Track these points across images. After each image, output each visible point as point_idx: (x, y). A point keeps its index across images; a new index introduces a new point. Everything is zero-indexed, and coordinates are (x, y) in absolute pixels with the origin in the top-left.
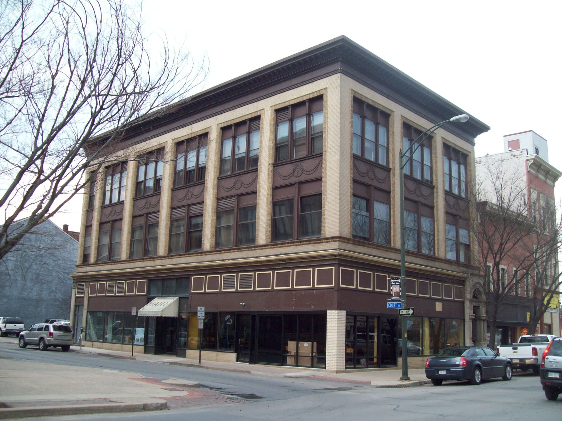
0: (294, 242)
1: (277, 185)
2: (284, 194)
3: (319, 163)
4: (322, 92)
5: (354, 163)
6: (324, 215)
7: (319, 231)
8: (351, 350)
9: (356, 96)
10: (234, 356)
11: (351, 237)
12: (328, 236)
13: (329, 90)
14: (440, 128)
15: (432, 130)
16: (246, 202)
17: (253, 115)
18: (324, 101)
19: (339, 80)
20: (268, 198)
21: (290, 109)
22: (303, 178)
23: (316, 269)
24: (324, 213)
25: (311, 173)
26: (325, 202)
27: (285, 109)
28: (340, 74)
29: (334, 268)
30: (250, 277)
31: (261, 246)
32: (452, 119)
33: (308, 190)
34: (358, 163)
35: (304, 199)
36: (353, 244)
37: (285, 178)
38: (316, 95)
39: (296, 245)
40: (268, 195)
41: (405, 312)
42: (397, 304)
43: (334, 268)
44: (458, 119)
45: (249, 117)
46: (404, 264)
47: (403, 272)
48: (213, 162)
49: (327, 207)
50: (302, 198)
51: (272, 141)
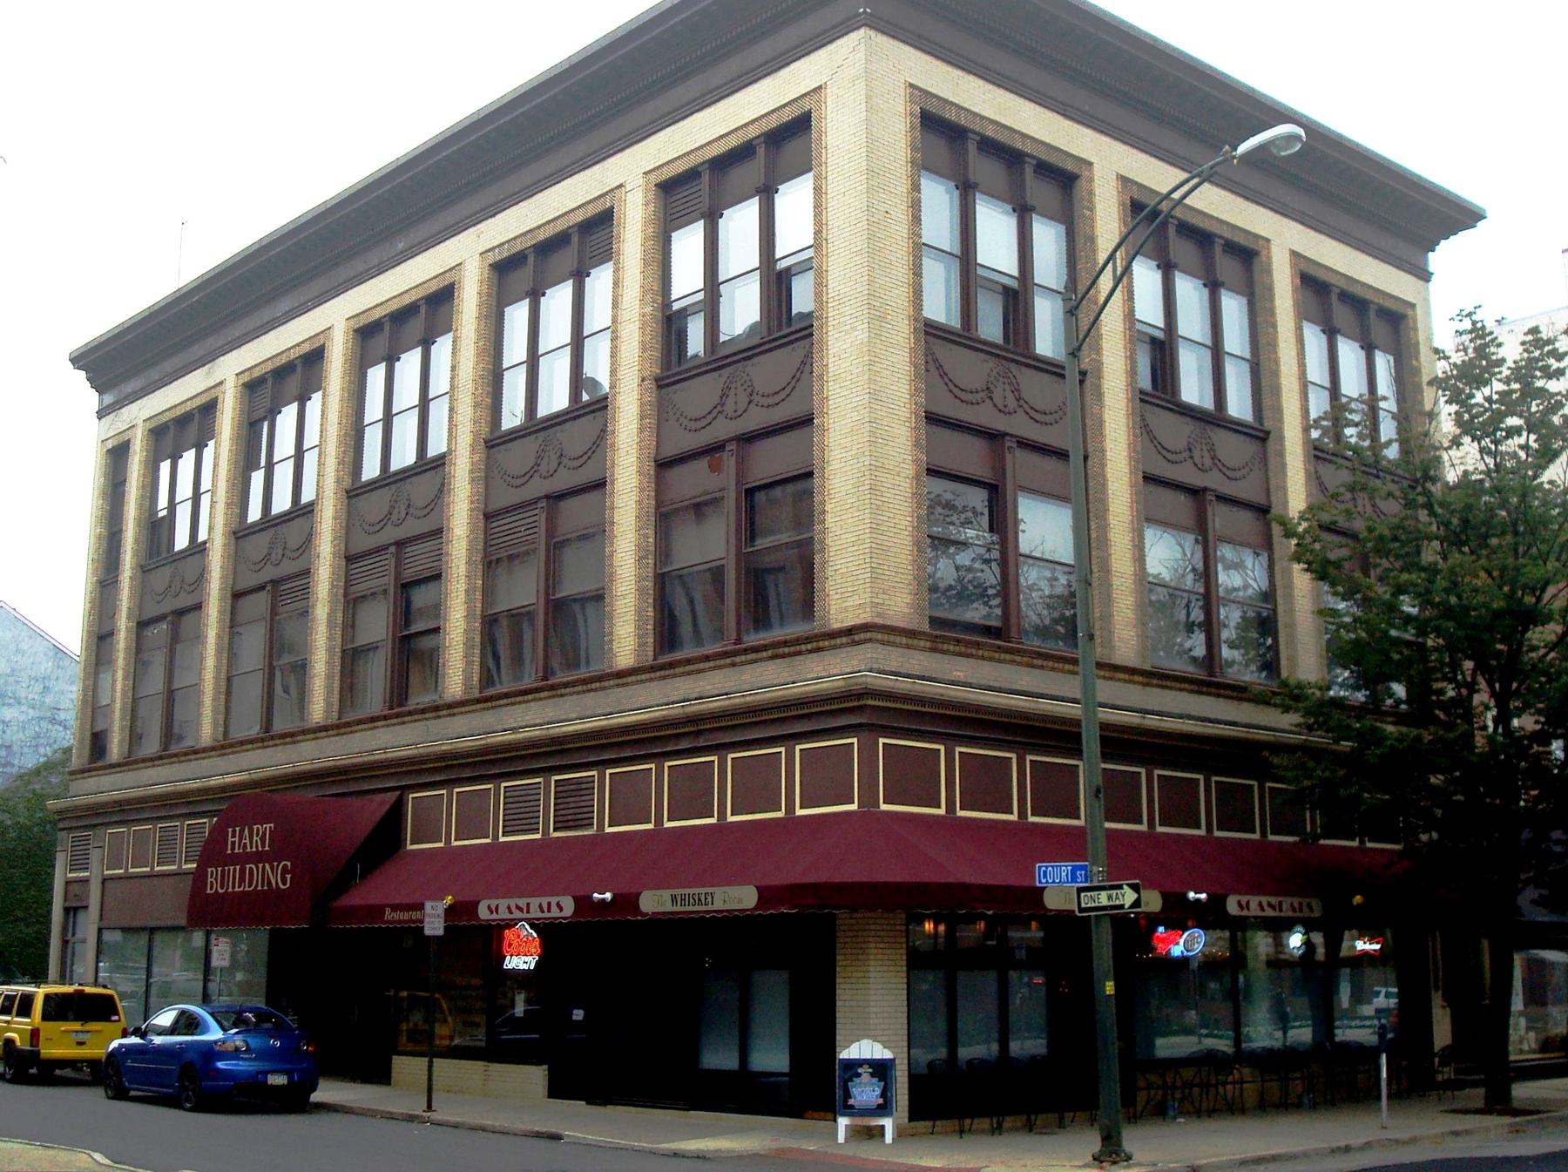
0: (726, 655)
1: (670, 451)
2: (693, 480)
3: (803, 363)
4: (807, 105)
5: (929, 354)
6: (823, 550)
7: (807, 605)
8: (71, 1015)
9: (933, 108)
10: (536, 1076)
11: (926, 627)
12: (836, 625)
13: (830, 95)
14: (1206, 185)
15: (1176, 195)
16: (574, 513)
17: (591, 211)
18: (814, 135)
19: (861, 55)
20: (640, 502)
21: (706, 177)
22: (756, 419)
23: (798, 748)
24: (822, 542)
25: (777, 399)
26: (823, 503)
27: (691, 175)
28: (862, 32)
29: (855, 740)
30: (583, 788)
31: (621, 674)
32: (1243, 148)
33: (770, 461)
34: (946, 352)
35: (761, 497)
36: (933, 650)
37: (694, 425)
38: (786, 116)
39: (733, 665)
40: (642, 490)
41: (1103, 898)
42: (1074, 869)
43: (855, 740)
44: (1263, 147)
45: (579, 217)
46: (1095, 713)
47: (1091, 742)
48: (470, 386)
49: (830, 520)
50: (750, 492)
51: (648, 298)
